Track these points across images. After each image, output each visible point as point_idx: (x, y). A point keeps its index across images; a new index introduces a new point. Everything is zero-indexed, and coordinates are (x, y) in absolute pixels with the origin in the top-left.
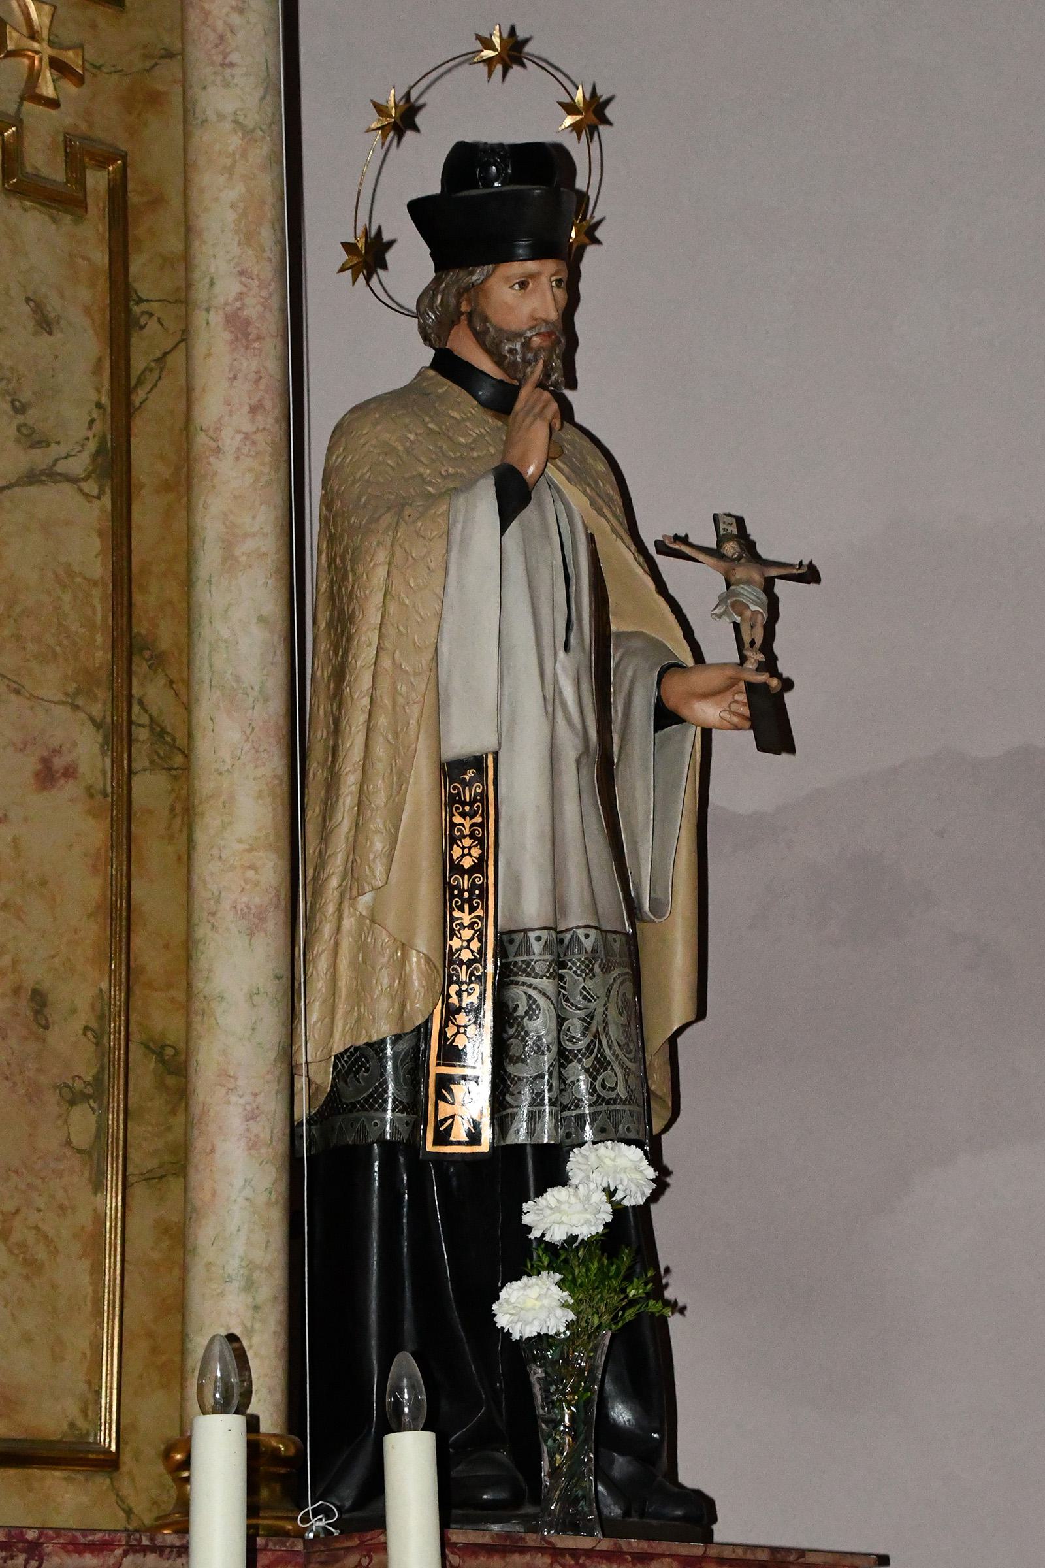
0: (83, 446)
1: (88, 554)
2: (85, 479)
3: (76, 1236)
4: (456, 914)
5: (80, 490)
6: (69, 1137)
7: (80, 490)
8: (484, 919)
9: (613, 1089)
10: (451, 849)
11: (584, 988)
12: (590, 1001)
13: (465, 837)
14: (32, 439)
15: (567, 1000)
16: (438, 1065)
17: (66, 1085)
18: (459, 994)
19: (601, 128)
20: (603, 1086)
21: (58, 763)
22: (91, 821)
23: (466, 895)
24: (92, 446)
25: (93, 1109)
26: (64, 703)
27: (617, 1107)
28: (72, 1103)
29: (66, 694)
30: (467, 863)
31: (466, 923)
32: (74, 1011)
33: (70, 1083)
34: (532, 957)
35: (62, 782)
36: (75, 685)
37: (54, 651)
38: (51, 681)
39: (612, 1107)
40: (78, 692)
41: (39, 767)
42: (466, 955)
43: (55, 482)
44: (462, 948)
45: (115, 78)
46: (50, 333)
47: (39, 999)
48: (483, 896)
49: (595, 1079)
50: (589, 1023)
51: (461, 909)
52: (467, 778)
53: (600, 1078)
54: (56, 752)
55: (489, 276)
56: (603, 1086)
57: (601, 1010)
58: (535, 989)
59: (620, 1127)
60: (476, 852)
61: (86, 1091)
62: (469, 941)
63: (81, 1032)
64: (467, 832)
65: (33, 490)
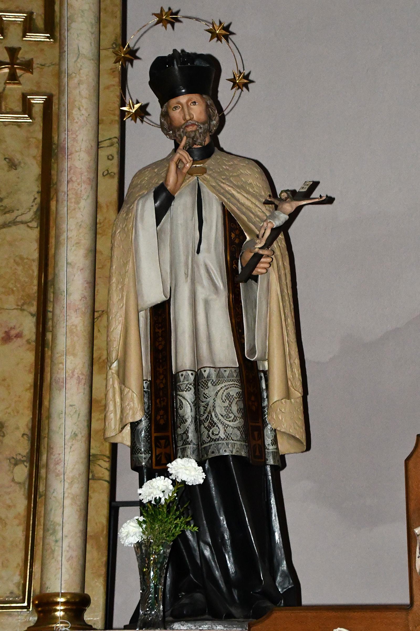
0: (30, 209)
1: (31, 250)
2: (30, 222)
3: (15, 518)
5: (28, 226)
6: (13, 478)
7: (28, 226)
9: (217, 435)
11: (204, 393)
12: (207, 398)
15: (200, 399)
17: (13, 458)
18: (160, 402)
19: (231, 36)
20: (213, 434)
21: (13, 333)
22: (28, 352)
24: (35, 208)
25: (26, 466)
26: (17, 309)
27: (220, 442)
28: (16, 464)
29: (18, 305)
30: (160, 348)
31: (161, 372)
32: (17, 428)
33: (15, 457)
34: (181, 383)
35: (15, 340)
36: (22, 301)
37: (13, 290)
38: (11, 301)
40: (23, 305)
41: (4, 335)
42: (162, 386)
43: (15, 225)
45: (51, 68)
46: (16, 169)
49: (209, 431)
50: (207, 408)
52: (160, 312)
53: (211, 431)
54: (14, 328)
55: (167, 107)
56: (213, 434)
58: (181, 396)
59: (221, 451)
60: (163, 343)
61: (22, 459)
62: (162, 380)
63: (21, 436)
64: (160, 335)
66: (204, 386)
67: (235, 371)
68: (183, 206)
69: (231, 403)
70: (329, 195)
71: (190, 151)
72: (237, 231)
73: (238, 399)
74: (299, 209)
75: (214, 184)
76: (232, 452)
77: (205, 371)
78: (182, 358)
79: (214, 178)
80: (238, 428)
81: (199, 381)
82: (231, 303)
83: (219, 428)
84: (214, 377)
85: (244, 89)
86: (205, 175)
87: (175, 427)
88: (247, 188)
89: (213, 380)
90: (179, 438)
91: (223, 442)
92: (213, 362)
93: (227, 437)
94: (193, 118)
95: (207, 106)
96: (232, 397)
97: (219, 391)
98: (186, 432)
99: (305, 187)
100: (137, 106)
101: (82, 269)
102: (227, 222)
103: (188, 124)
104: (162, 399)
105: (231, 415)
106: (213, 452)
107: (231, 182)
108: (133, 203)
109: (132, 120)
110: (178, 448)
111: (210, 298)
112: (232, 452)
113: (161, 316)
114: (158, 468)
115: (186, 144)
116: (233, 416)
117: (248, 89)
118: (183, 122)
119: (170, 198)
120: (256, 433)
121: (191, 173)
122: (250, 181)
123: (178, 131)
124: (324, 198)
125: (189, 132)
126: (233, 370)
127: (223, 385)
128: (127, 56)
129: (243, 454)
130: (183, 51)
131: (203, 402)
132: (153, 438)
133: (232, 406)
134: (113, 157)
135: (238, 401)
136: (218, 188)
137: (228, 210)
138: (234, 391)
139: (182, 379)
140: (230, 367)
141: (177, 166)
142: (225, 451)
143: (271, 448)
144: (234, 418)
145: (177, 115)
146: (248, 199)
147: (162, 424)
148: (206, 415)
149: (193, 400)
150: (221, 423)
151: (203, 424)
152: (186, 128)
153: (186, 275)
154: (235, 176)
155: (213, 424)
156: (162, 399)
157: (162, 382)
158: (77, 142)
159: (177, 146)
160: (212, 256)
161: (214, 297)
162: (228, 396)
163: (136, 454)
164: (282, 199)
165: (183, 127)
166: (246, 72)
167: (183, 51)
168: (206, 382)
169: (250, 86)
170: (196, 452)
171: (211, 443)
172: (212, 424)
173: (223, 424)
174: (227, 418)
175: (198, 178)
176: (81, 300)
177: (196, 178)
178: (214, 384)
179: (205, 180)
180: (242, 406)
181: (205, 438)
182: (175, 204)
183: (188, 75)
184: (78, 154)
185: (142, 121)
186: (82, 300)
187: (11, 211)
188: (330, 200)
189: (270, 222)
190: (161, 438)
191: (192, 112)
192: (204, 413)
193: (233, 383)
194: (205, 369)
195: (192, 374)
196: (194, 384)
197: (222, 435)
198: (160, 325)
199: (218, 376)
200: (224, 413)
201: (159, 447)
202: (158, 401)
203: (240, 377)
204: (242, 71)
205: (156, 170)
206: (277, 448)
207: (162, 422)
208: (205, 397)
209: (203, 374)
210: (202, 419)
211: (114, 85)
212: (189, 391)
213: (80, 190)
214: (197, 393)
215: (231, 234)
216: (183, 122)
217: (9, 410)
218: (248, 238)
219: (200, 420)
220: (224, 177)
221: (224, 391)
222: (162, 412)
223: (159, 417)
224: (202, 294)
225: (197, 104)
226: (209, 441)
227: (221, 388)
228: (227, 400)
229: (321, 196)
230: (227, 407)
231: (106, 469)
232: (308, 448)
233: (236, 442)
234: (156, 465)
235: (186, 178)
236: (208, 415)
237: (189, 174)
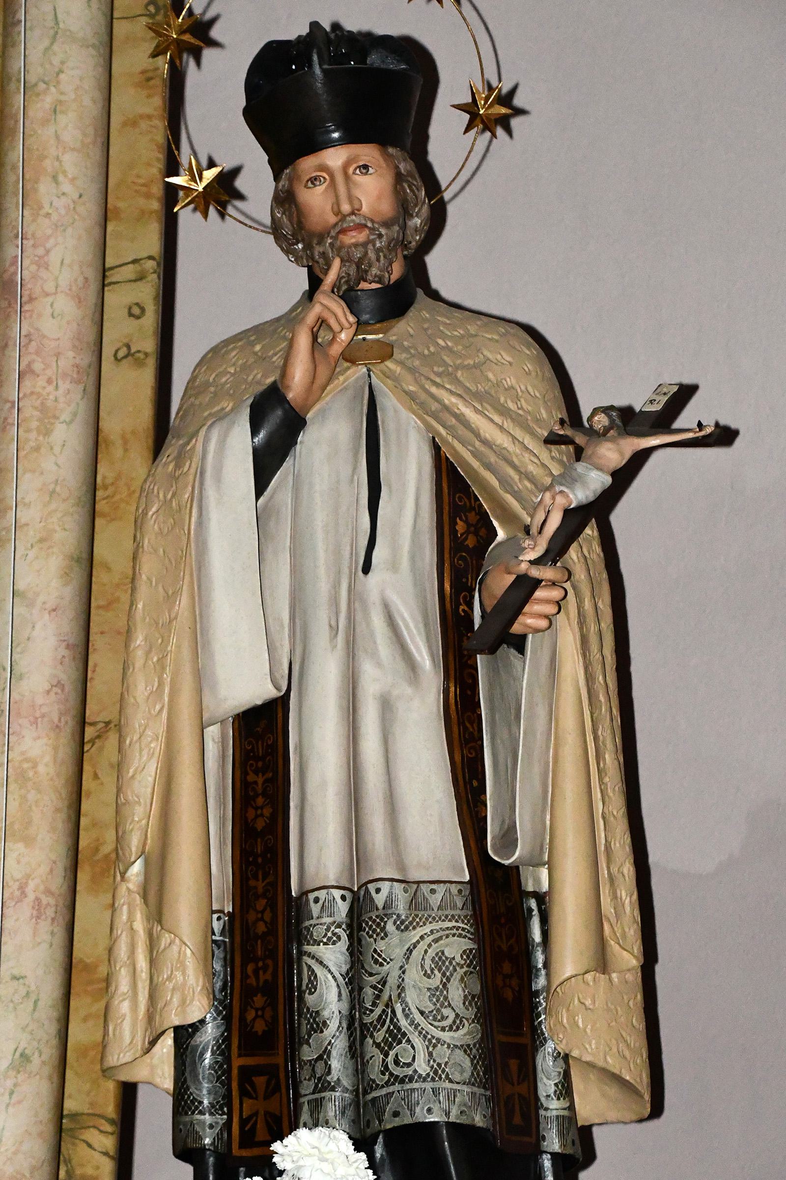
4: (252, 883)
9: (409, 1065)
10: (246, 812)
11: (375, 951)
12: (381, 965)
13: (257, 796)
15: (363, 967)
16: (240, 1056)
18: (256, 972)
20: (397, 1062)
23: (260, 860)
27: (415, 1085)
30: (260, 824)
31: (260, 890)
34: (312, 922)
39: (408, 1086)
44: (258, 920)
49: (386, 1055)
50: (381, 991)
51: (256, 878)
53: (392, 1053)
55: (291, 180)
56: (397, 1062)
57: (396, 973)
58: (313, 957)
59: (418, 1110)
60: (267, 812)
62: (263, 912)
64: (260, 789)
66: (374, 931)
67: (460, 891)
68: (327, 445)
69: (448, 980)
70: (722, 422)
71: (349, 296)
72: (473, 513)
73: (465, 969)
74: (640, 458)
75: (412, 388)
76: (448, 1114)
77: (378, 891)
78: (319, 854)
79: (412, 370)
80: (466, 1049)
81: (362, 919)
82: (453, 707)
83: (413, 1047)
84: (401, 907)
85: (500, 131)
86: (389, 364)
87: (295, 1042)
88: (502, 400)
89: (399, 916)
90: (306, 1073)
91: (423, 1085)
92: (401, 866)
93: (436, 1072)
94: (359, 210)
95: (399, 178)
96: (451, 963)
97: (415, 947)
98: (324, 1056)
99: (658, 398)
100: (209, 175)
101: (54, 610)
102: (446, 490)
103: (345, 225)
104: (260, 964)
105: (446, 1012)
106: (396, 1114)
107: (457, 381)
108: (196, 434)
109: (195, 210)
110: (302, 1100)
111: (395, 692)
112: (448, 1114)
113: (262, 739)
114: (245, 1153)
115: (339, 278)
116: (452, 1016)
117: (509, 131)
118: (333, 219)
119: (294, 424)
120: (513, 1064)
121: (350, 356)
122: (510, 381)
123: (319, 243)
124: (708, 430)
125: (350, 247)
126: (454, 889)
127: (427, 929)
128: (187, 37)
129: (479, 1120)
130: (336, 26)
131: (371, 975)
132: (235, 1072)
133: (449, 986)
134: (143, 310)
135: (465, 973)
136: (423, 396)
137: (447, 458)
138: (456, 948)
139: (315, 909)
140: (444, 882)
141: (315, 337)
142: (429, 1111)
143: (554, 1106)
144: (454, 1022)
145: (316, 201)
146: (501, 428)
147: (260, 1033)
148: (378, 1011)
149: (344, 969)
150: (420, 1033)
151: (372, 1036)
152: (341, 236)
153: (334, 630)
154: (467, 368)
155: (397, 1036)
156: (260, 964)
157: (262, 919)
158: (47, 269)
159: (315, 282)
160: (404, 581)
161: (409, 691)
162: (440, 960)
163: (186, 1114)
164: (596, 431)
165: (333, 233)
166: (506, 88)
167: (336, 26)
168: (382, 919)
169: (515, 122)
170: (350, 1113)
171: (391, 1089)
172: (394, 1038)
173: (425, 1037)
174: (435, 1019)
175: (369, 370)
176: (48, 692)
177: (365, 370)
178: (403, 927)
179: (388, 375)
180: (477, 989)
181: (374, 1073)
182: (306, 439)
183: (348, 92)
184: (50, 299)
185: (222, 215)
186: (52, 694)
188: (724, 436)
189: (561, 492)
190: (258, 1070)
191: (357, 193)
192: (374, 1004)
193: (454, 924)
194: (380, 884)
195: (343, 898)
196: (350, 926)
197: (422, 1066)
198: (260, 764)
199: (415, 903)
200: (428, 1007)
201: (251, 1097)
202: (250, 968)
203: (474, 909)
204: (495, 83)
205: (258, 348)
206: (572, 1108)
207: (260, 1027)
208: (376, 961)
209: (372, 900)
210: (367, 1020)
211: (149, 117)
212: (334, 943)
213: (51, 397)
214: (355, 951)
215: (456, 523)
216: (333, 219)
218: (501, 535)
219: (363, 1025)
220: (441, 369)
221: (430, 946)
222: (259, 1000)
223: (251, 1015)
224: (374, 680)
225: (371, 170)
226: (387, 1083)
227: (422, 937)
228: (436, 972)
229: (700, 425)
230: (437, 989)
231: (106, 1154)
232: (657, 1109)
233: (455, 1086)
234: (242, 1146)
235: (338, 369)
236: (384, 1011)
237: (347, 360)
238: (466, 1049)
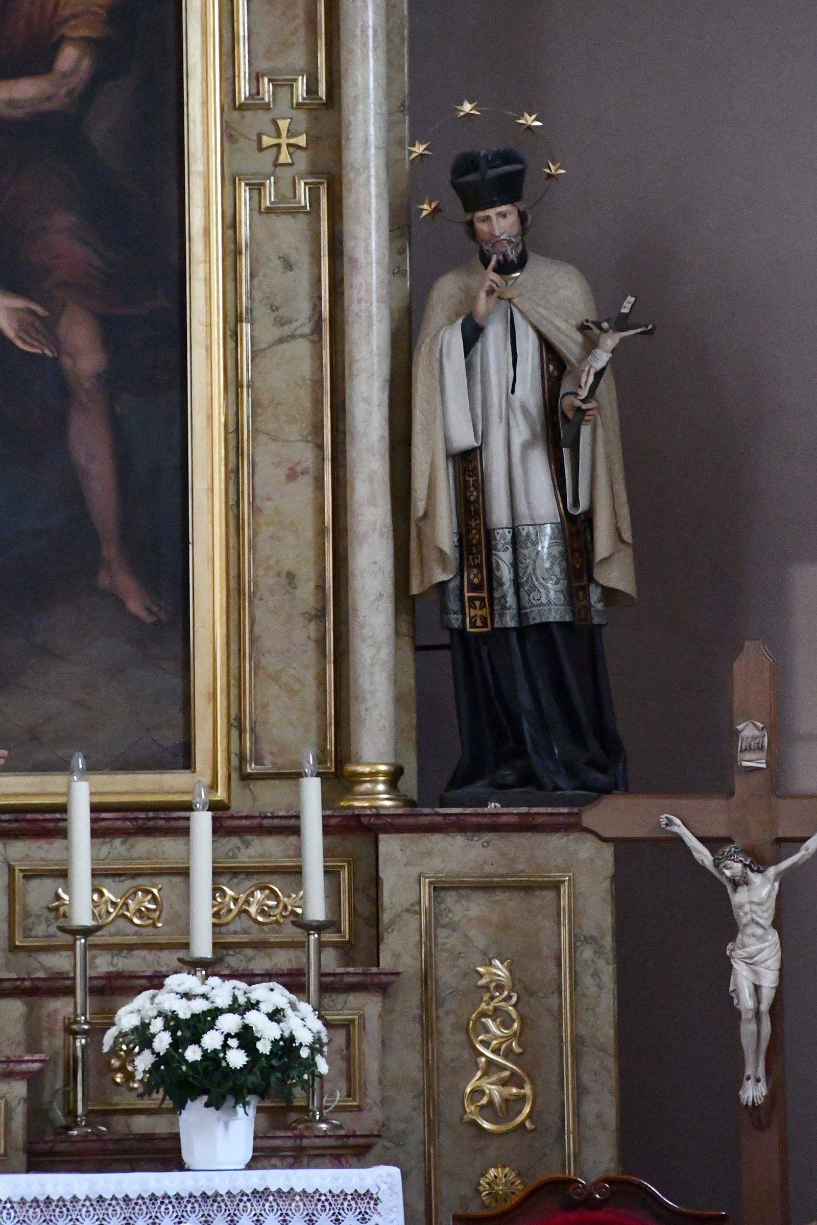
8: (479, 524)
14: (281, 322)
18: (473, 559)
21: (299, 469)
37: (295, 418)
46: (292, 270)
47: (291, 577)
48: (478, 514)
54: (299, 463)
65: (281, 347)
68: (494, 337)
80: (562, 592)
92: (532, 519)
98: (504, 596)
120: (581, 594)
129: (567, 619)
132: (466, 598)
139: (498, 538)
170: (516, 618)
180: (564, 565)
187: (289, 322)
190: (477, 598)
197: (544, 600)
202: (471, 557)
207: (476, 581)
217: (300, 558)
223: (472, 576)
238: (562, 592)
